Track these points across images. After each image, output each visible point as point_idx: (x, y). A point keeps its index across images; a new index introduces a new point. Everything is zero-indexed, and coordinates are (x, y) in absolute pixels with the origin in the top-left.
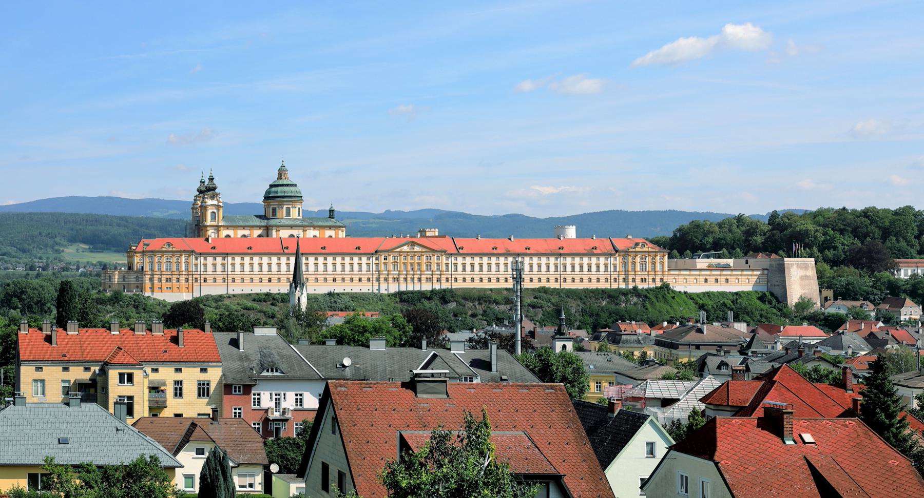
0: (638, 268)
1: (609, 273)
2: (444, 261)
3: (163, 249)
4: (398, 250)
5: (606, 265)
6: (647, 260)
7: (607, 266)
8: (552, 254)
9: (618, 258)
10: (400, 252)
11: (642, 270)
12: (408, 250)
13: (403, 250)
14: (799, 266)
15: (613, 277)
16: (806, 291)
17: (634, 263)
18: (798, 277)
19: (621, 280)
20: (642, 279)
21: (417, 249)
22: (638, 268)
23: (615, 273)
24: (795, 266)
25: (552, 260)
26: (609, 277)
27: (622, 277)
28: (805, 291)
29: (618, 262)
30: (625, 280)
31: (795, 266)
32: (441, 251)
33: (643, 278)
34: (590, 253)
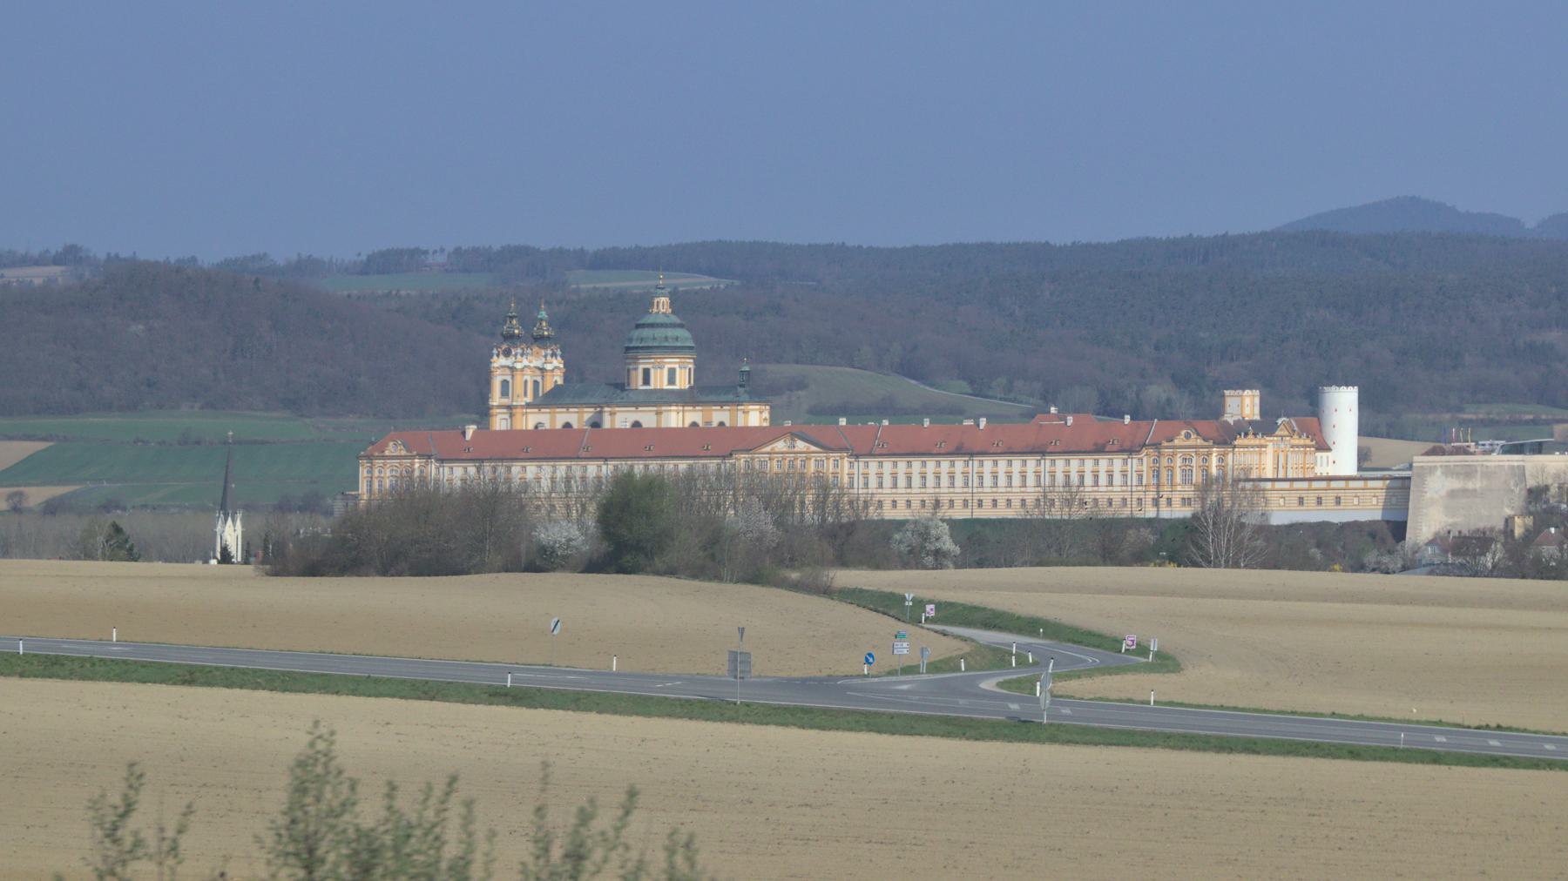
0: (1178, 479)
1: (1129, 489)
2: (846, 471)
3: (387, 453)
4: (768, 449)
5: (1124, 474)
6: (1194, 464)
7: (1142, 475)
8: (1031, 453)
9: (1145, 459)
10: (768, 453)
11: (1184, 482)
12: (785, 449)
13: (777, 450)
14: (1448, 472)
15: (1135, 496)
16: (1458, 520)
17: (1171, 469)
18: (1443, 492)
19: (1149, 502)
20: (1183, 499)
21: (801, 445)
22: (1178, 479)
23: (1140, 488)
24: (1439, 472)
25: (1031, 462)
26: (1127, 496)
27: (1151, 495)
28: (1455, 520)
29: (1145, 468)
30: (1156, 502)
31: (1439, 472)
32: (841, 450)
33: (1186, 496)
34: (1099, 449)
